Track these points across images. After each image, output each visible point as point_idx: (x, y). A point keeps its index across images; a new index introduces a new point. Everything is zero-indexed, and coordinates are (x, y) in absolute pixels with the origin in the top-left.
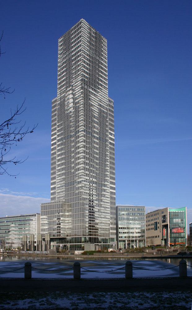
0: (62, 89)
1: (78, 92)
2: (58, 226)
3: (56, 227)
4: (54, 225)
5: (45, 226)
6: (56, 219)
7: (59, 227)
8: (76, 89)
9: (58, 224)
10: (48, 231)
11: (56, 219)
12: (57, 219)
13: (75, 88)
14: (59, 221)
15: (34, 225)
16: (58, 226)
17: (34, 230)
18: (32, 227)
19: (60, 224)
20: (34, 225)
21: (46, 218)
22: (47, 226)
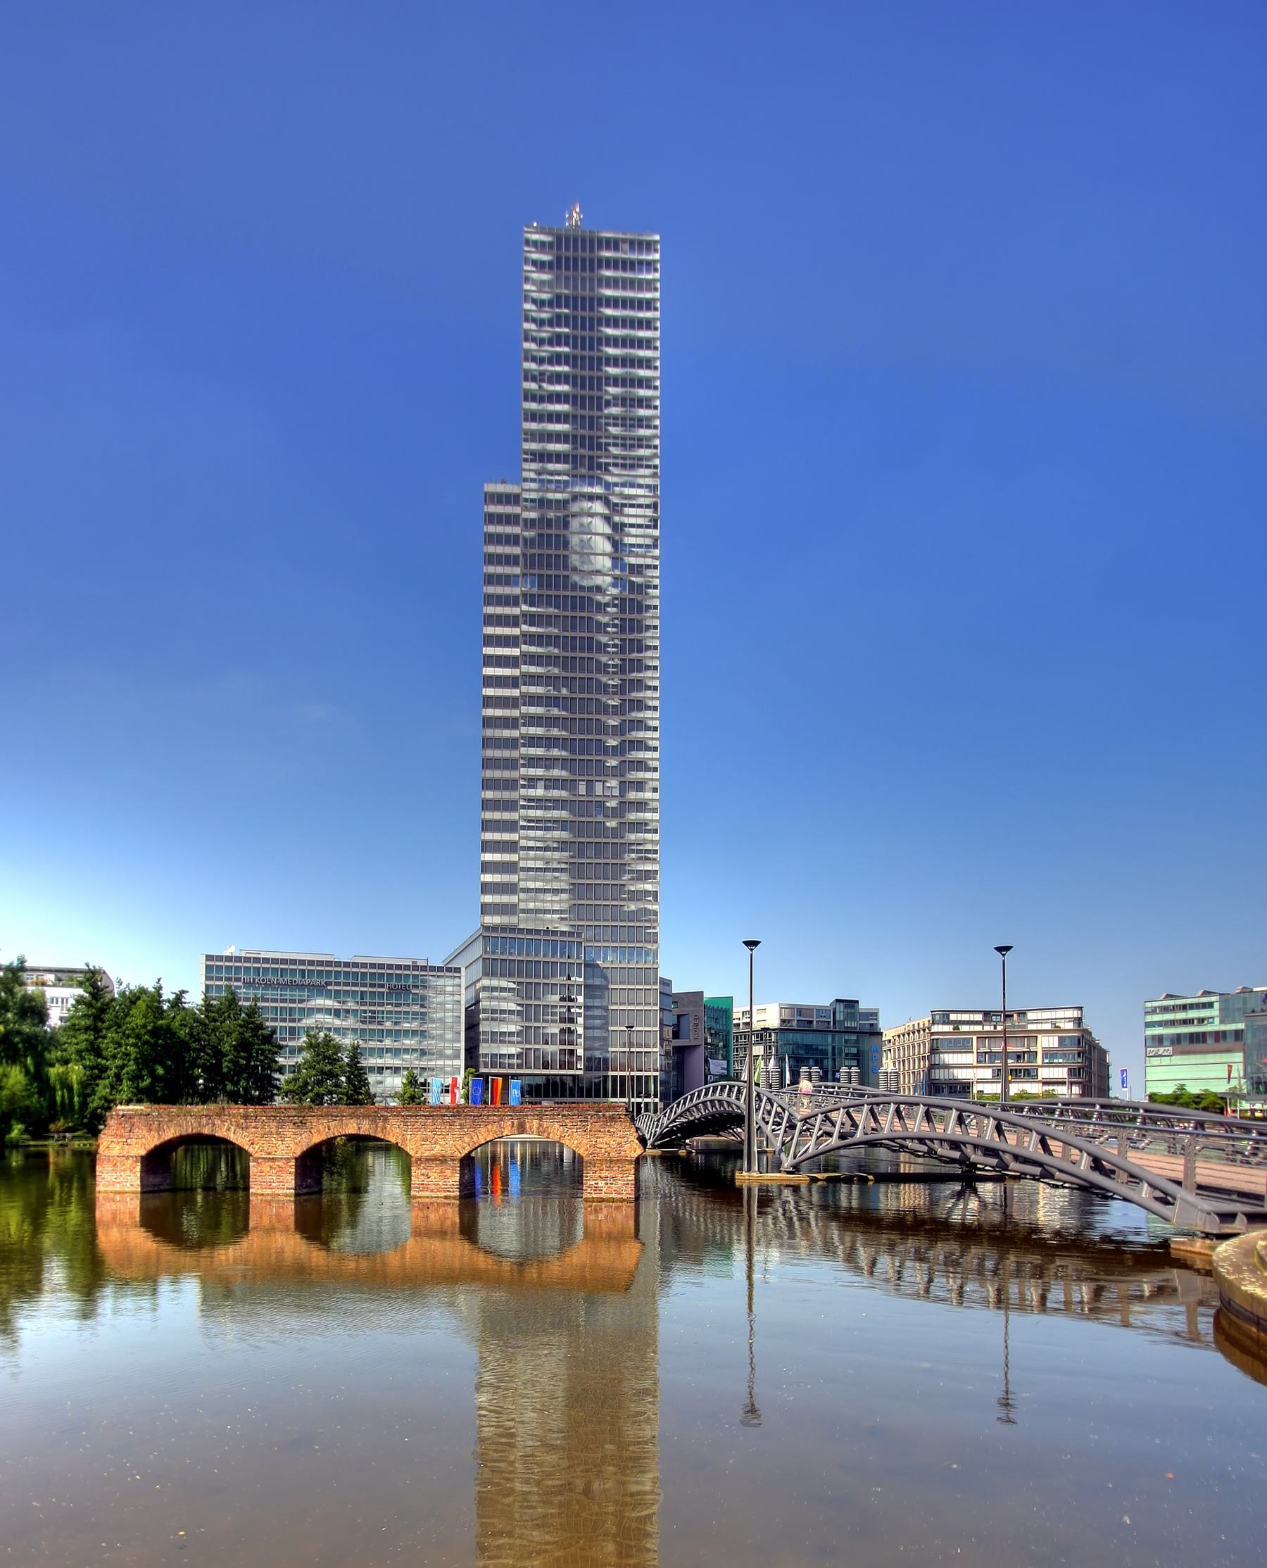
0: (551, 466)
1: (640, 531)
3: (557, 1031)
4: (547, 1021)
5: (503, 1020)
6: (557, 997)
7: (571, 1032)
8: (626, 510)
9: (562, 1020)
10: (521, 1043)
11: (554, 999)
12: (562, 999)
13: (624, 505)
14: (569, 1008)
15: (449, 1010)
17: (449, 1036)
18: (442, 1020)
19: (572, 1021)
20: (449, 1010)
21: (511, 990)
22: (515, 1023)
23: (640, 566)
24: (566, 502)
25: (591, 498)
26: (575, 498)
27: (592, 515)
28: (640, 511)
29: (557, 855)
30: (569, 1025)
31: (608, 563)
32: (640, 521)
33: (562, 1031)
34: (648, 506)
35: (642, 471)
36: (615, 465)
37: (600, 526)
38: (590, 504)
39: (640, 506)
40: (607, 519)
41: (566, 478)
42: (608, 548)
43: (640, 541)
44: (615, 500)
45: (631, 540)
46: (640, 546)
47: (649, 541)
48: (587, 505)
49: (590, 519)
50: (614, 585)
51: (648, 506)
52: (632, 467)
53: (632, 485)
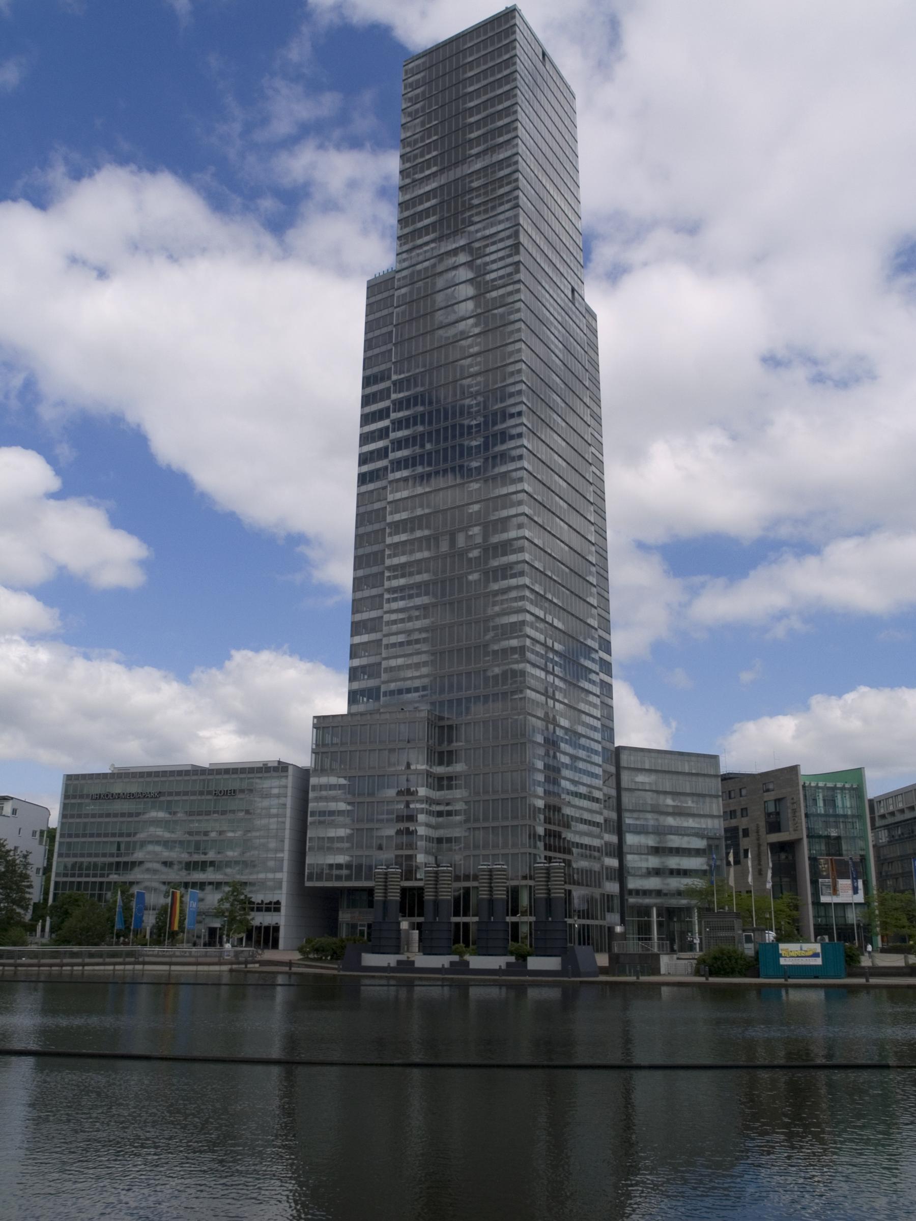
1: (501, 264)
2: (402, 826)
3: (391, 832)
4: (381, 821)
8: (488, 250)
9: (400, 819)
13: (487, 246)
16: (402, 826)
23: (503, 296)
24: (434, 266)
25: (455, 252)
26: (441, 257)
27: (455, 268)
28: (501, 245)
29: (418, 624)
30: (407, 825)
31: (470, 305)
32: (501, 254)
33: (399, 832)
34: (508, 237)
35: (502, 209)
36: (478, 213)
37: (464, 274)
38: (454, 259)
39: (502, 240)
40: (469, 264)
41: (433, 245)
42: (470, 291)
43: (501, 273)
44: (476, 245)
45: (493, 275)
46: (501, 277)
47: (509, 270)
48: (451, 261)
49: (454, 273)
50: (476, 325)
51: (508, 237)
52: (494, 208)
53: (492, 225)
